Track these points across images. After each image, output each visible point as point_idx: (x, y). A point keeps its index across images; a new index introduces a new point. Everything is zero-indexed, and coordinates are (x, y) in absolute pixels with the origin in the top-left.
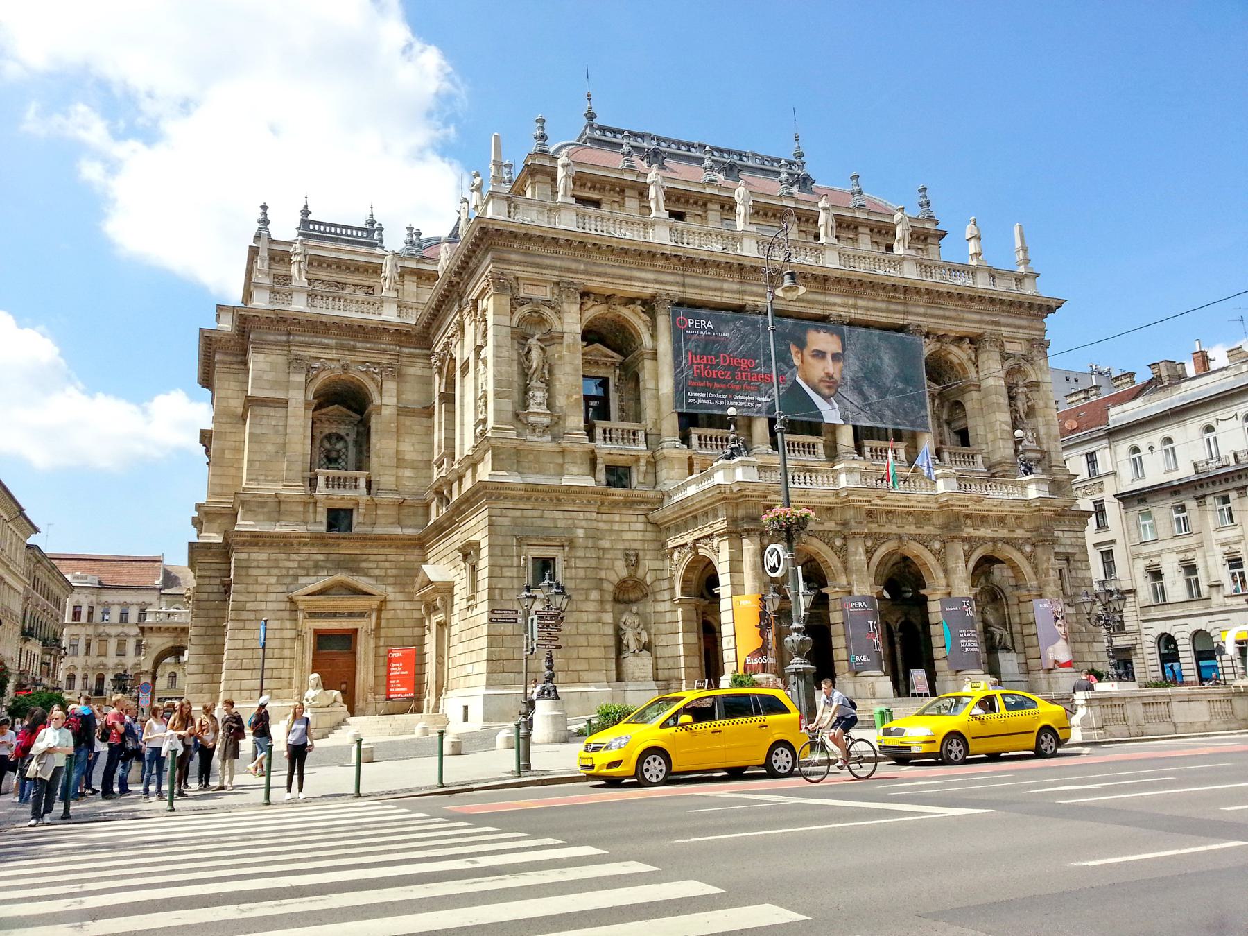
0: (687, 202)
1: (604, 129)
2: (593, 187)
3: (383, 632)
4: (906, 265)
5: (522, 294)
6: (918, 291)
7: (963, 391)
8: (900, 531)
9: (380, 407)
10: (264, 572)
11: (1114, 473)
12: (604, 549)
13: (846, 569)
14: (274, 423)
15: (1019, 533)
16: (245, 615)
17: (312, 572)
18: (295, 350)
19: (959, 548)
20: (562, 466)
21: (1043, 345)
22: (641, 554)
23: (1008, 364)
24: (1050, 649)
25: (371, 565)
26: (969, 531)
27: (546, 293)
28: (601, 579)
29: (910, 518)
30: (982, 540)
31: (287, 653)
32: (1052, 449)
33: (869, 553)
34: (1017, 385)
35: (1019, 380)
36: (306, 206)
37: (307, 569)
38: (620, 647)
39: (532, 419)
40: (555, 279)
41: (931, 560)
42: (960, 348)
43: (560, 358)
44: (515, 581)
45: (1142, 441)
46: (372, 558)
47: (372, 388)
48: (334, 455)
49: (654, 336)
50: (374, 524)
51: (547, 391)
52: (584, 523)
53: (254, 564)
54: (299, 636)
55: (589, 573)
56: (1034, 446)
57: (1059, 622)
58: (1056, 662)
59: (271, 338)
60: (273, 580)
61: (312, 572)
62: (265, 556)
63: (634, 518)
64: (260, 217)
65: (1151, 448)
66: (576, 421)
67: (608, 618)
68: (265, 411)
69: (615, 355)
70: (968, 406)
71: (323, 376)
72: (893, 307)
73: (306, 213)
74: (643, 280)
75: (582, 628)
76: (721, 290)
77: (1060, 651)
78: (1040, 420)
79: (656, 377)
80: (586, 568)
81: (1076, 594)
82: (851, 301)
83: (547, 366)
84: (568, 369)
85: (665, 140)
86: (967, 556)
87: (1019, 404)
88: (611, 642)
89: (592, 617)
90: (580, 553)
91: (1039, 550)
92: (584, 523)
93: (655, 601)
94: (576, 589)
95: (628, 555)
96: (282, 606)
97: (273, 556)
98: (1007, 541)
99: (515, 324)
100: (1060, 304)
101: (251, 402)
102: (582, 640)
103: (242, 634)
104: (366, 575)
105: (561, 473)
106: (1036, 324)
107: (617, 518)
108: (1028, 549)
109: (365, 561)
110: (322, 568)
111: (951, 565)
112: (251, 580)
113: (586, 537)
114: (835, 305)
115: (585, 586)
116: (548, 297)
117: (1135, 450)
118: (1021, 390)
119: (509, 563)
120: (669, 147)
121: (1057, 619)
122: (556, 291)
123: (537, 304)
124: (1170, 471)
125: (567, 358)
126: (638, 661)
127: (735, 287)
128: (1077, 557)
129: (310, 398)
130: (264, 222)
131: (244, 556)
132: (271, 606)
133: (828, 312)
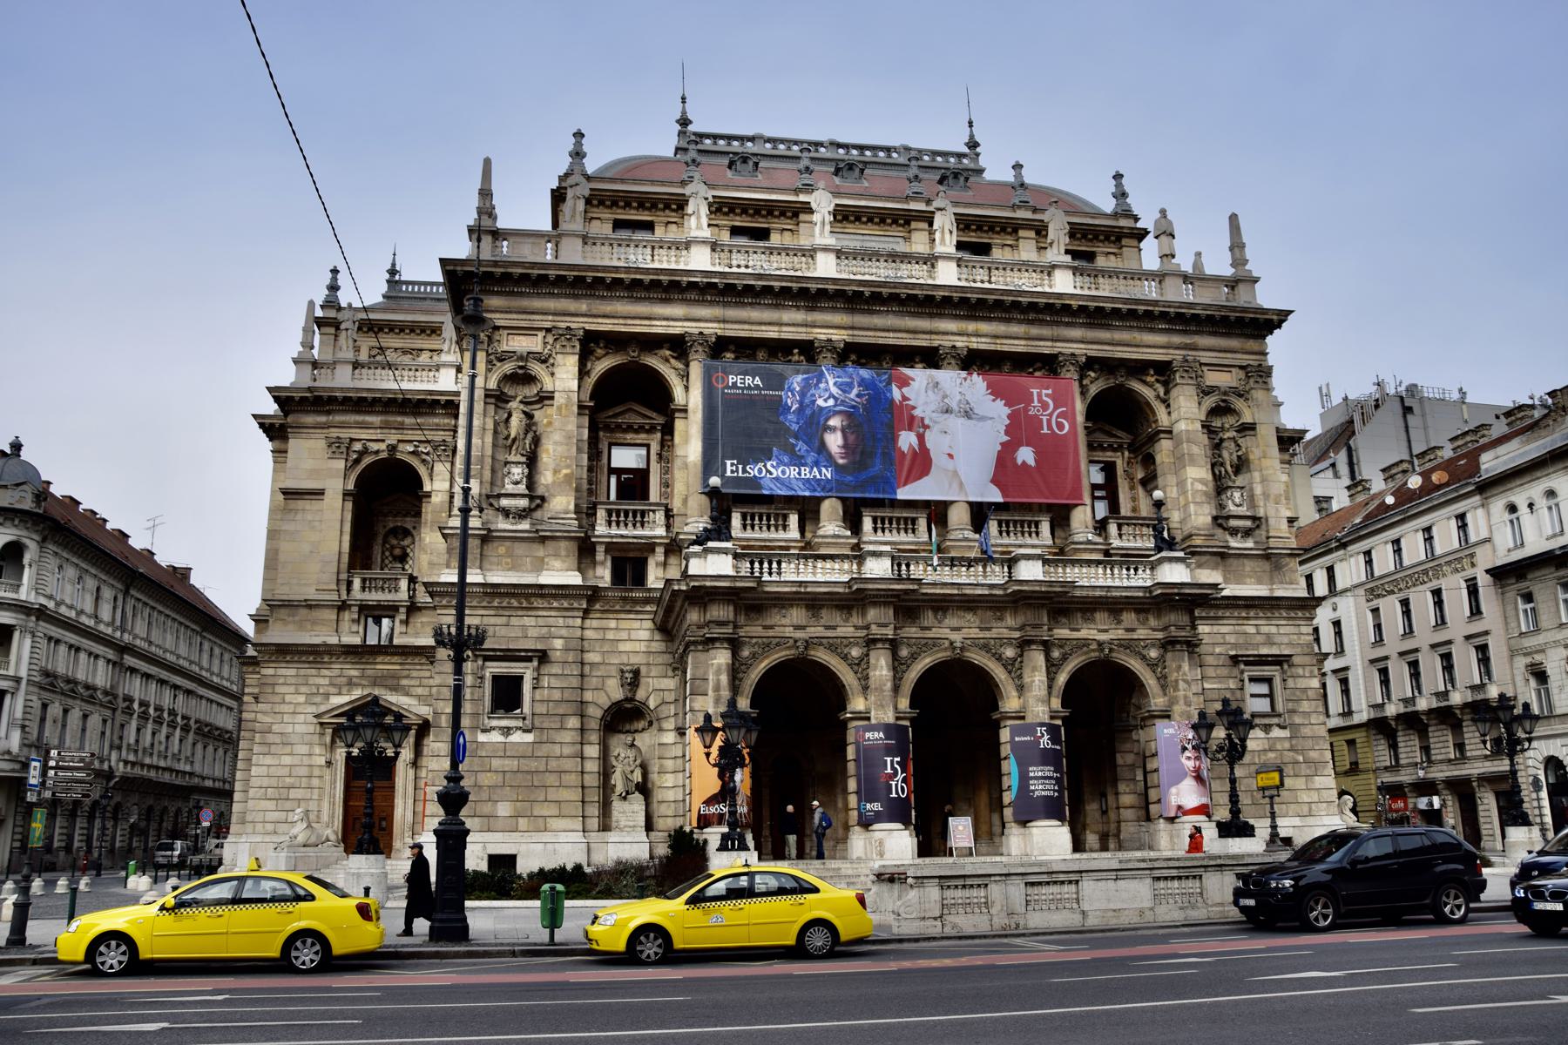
0: (770, 213)
1: (702, 136)
2: (641, 206)
3: (424, 761)
4: (1058, 274)
5: (505, 348)
6: (1066, 309)
7: (1154, 438)
8: (957, 637)
9: (429, 495)
10: (292, 689)
11: (1488, 540)
13: (865, 688)
14: (309, 517)
15: (1142, 633)
16: (270, 738)
17: (344, 690)
18: (334, 433)
19: (1037, 658)
20: (542, 559)
21: (1261, 374)
22: (643, 670)
23: (1210, 402)
24: (1173, 790)
25: (413, 682)
26: (1062, 633)
27: (533, 344)
29: (969, 616)
30: (1085, 643)
31: (315, 782)
32: (1271, 513)
33: (898, 667)
34: (1222, 428)
35: (1230, 421)
36: (394, 265)
37: (340, 687)
38: (606, 787)
39: (504, 502)
40: (548, 325)
41: (999, 673)
42: (1144, 382)
43: (550, 423)
45: (1520, 497)
46: (414, 674)
47: (422, 471)
48: (397, 552)
49: (687, 388)
50: (417, 635)
51: (528, 466)
53: (281, 681)
54: (329, 763)
55: (567, 695)
56: (1243, 511)
57: (1187, 754)
58: (1180, 807)
59: (309, 419)
60: (302, 699)
61: (344, 690)
62: (292, 672)
63: (637, 624)
64: (328, 282)
65: (1531, 506)
66: (562, 504)
67: (593, 751)
68: (300, 504)
69: (654, 415)
70: (1158, 459)
71: (367, 460)
72: (1035, 331)
73: (393, 272)
75: (553, 764)
76: (781, 325)
77: (1186, 794)
78: (1256, 475)
79: (686, 441)
81: (1293, 711)
82: (971, 326)
83: (530, 436)
84: (557, 437)
85: (782, 141)
86: (1052, 668)
87: (1225, 454)
88: (592, 780)
89: (567, 750)
90: (556, 669)
91: (1169, 655)
92: (564, 632)
93: (661, 730)
95: (622, 671)
96: (311, 729)
97: (302, 672)
98: (1127, 645)
99: (492, 385)
100: (1284, 315)
101: (289, 494)
102: (551, 779)
103: (268, 760)
104: (407, 694)
105: (540, 565)
106: (1252, 344)
107: (613, 624)
108: (1153, 653)
109: (407, 677)
110: (357, 685)
111: (1027, 680)
112: (277, 699)
113: (566, 650)
114: (946, 333)
115: (561, 711)
116: (539, 349)
117: (1512, 508)
118: (1227, 435)
120: (789, 148)
121: (1184, 749)
122: (550, 339)
123: (521, 358)
124: (1554, 536)
125: (557, 424)
126: (625, 806)
127: (799, 316)
128: (1296, 660)
129: (351, 486)
130: (334, 288)
131: (270, 671)
132: (299, 729)
133: (936, 344)
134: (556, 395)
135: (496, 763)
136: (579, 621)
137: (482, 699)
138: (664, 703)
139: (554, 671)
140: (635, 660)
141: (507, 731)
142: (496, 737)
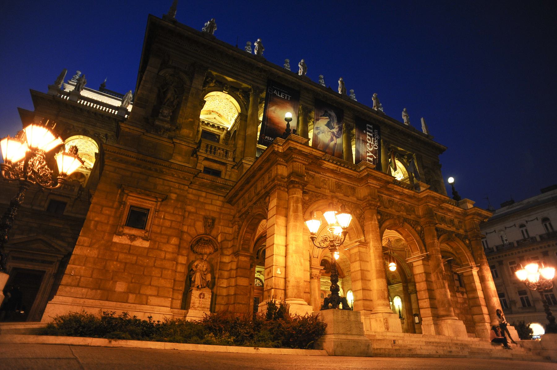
12: (190, 213)
13: (364, 231)
28: (182, 232)
38: (189, 284)
39: (157, 123)
44: (111, 219)
52: (177, 191)
63: (216, 197)
67: (182, 260)
74: (244, 77)
75: (158, 263)
80: (172, 221)
88: (180, 278)
89: (168, 256)
90: (170, 210)
92: (177, 191)
93: (222, 254)
94: (161, 234)
107: (204, 194)
115: (169, 232)
119: (111, 204)
134: (192, 89)
135: (122, 256)
136: (187, 187)
137: (120, 217)
138: (225, 240)
139: (168, 210)
140: (213, 215)
141: (133, 238)
142: (124, 240)
